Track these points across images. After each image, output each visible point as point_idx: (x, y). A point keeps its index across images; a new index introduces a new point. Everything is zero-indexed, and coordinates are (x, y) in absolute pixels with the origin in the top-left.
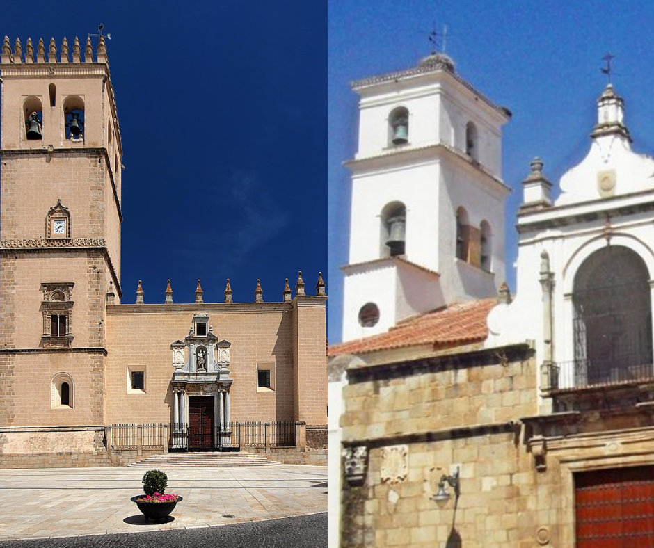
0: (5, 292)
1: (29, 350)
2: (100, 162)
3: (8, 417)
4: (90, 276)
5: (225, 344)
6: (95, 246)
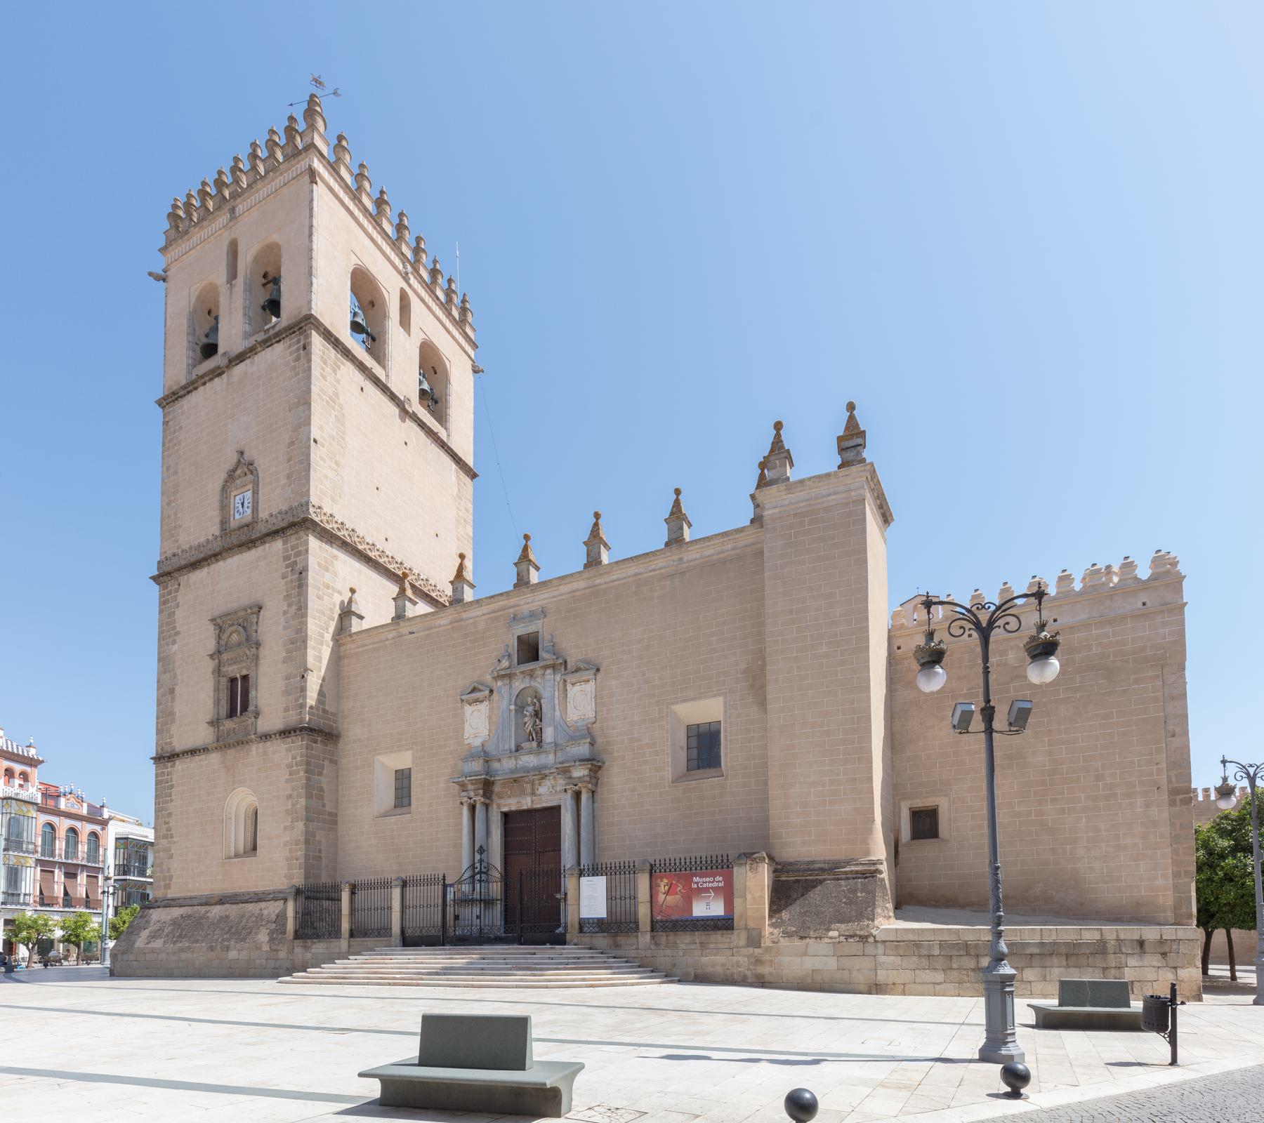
4: (286, 584)
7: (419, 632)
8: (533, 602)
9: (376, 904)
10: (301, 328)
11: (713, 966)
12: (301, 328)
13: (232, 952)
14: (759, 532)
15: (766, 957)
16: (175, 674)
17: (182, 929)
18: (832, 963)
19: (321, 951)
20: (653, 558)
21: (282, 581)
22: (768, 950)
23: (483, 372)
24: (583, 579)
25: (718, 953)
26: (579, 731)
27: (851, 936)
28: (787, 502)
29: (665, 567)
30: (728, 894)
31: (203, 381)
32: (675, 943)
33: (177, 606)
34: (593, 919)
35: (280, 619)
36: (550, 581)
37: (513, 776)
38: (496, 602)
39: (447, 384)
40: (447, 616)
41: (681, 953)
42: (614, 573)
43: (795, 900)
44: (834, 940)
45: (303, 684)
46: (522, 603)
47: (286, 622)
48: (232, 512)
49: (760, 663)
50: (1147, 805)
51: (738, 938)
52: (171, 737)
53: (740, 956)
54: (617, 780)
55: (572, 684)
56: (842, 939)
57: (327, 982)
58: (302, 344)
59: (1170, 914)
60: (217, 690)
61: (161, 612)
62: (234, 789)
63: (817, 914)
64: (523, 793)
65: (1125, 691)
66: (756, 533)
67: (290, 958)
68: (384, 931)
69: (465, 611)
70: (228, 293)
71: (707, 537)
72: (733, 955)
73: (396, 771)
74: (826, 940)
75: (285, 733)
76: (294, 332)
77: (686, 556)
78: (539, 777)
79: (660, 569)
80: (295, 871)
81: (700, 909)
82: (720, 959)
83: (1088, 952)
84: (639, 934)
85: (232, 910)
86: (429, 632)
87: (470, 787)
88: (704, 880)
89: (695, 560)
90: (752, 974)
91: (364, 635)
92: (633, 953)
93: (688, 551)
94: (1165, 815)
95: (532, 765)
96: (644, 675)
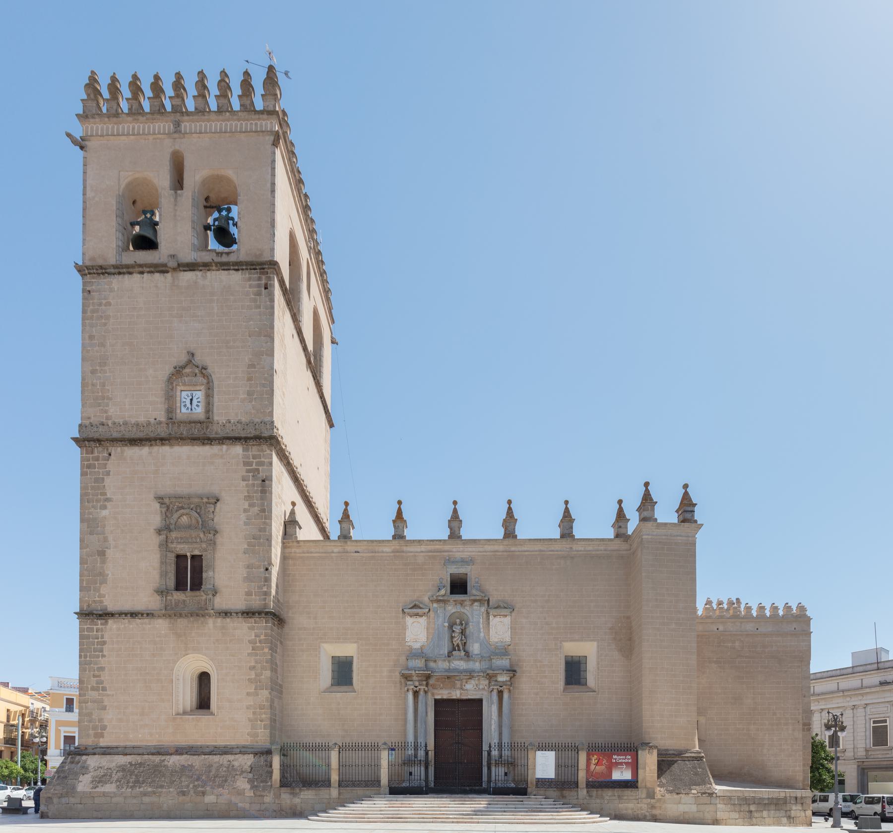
0: (90, 513)
2: (266, 288)
3: (95, 728)
4: (247, 486)
5: (505, 607)
7: (363, 552)
8: (463, 552)
9: (363, 760)
10: (264, 269)
11: (626, 809)
12: (264, 269)
13: (209, 797)
14: (622, 544)
15: (658, 805)
16: (106, 540)
17: (136, 776)
18: (694, 808)
19: (310, 797)
20: (554, 543)
21: (242, 482)
22: (659, 800)
23: (337, 344)
24: (503, 545)
25: (630, 802)
26: (499, 649)
27: (704, 793)
28: (655, 533)
29: (561, 551)
30: (635, 767)
31: (141, 269)
32: (602, 795)
34: (548, 779)
35: (240, 515)
36: (479, 540)
37: (448, 674)
38: (433, 545)
39: (321, 346)
40: (390, 546)
41: (606, 802)
42: (526, 546)
43: (666, 771)
44: (695, 795)
45: (267, 575)
46: (454, 550)
47: (247, 519)
49: (619, 625)
50: (794, 730)
51: (642, 793)
53: (642, 804)
54: (526, 685)
55: (494, 616)
56: (699, 794)
57: (393, 821)
58: (263, 282)
59: (801, 784)
60: (163, 563)
62: (187, 655)
63: (681, 780)
64: (453, 687)
65: (786, 671)
66: (620, 544)
67: (276, 802)
68: (374, 783)
69: (406, 546)
70: (172, 200)
71: (592, 539)
72: (638, 803)
73: (332, 657)
74: (691, 795)
75: (248, 614)
76: (255, 269)
77: (575, 547)
78: (468, 677)
79: (557, 551)
80: (260, 730)
81: (617, 775)
82: (631, 805)
83: (782, 802)
84: (579, 789)
85: (196, 761)
86: (373, 554)
87: (415, 678)
88: (620, 757)
89: (581, 551)
90: (649, 814)
91: (311, 544)
92: (575, 802)
93: (577, 544)
94: (801, 736)
95: (462, 668)
96: (545, 619)
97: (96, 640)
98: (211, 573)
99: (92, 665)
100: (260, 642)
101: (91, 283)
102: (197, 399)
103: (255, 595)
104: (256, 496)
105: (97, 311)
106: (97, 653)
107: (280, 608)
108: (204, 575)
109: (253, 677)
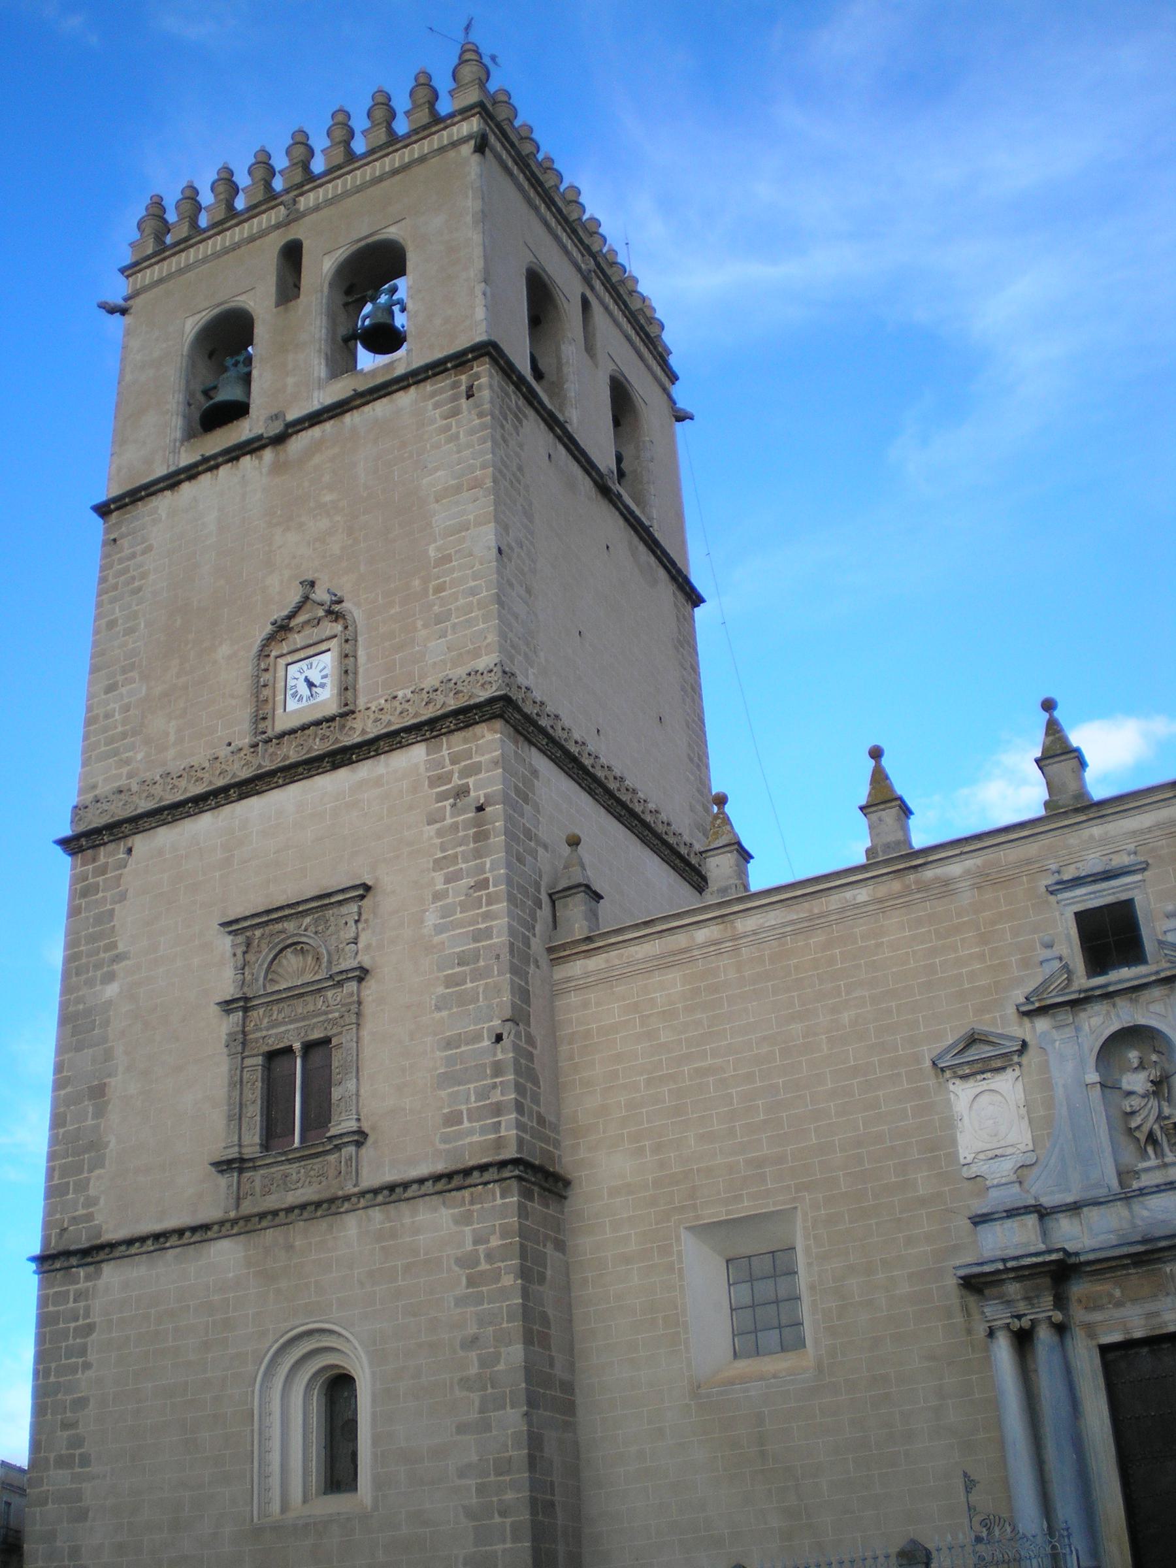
1: (157, 1237)
4: (439, 833)
6: (453, 704)
16: (108, 1055)
33: (123, 897)
48: (280, 698)
52: (91, 1202)
60: (237, 1083)
61: (74, 912)
80: (499, 1547)
97: (73, 1325)
98: (351, 1085)
99: (59, 1396)
100: (489, 1257)
101: (118, 524)
102: (321, 671)
103: (470, 1120)
104: (463, 852)
105: (126, 570)
106: (74, 1360)
107: (546, 1140)
108: (336, 1093)
109: (474, 1370)
